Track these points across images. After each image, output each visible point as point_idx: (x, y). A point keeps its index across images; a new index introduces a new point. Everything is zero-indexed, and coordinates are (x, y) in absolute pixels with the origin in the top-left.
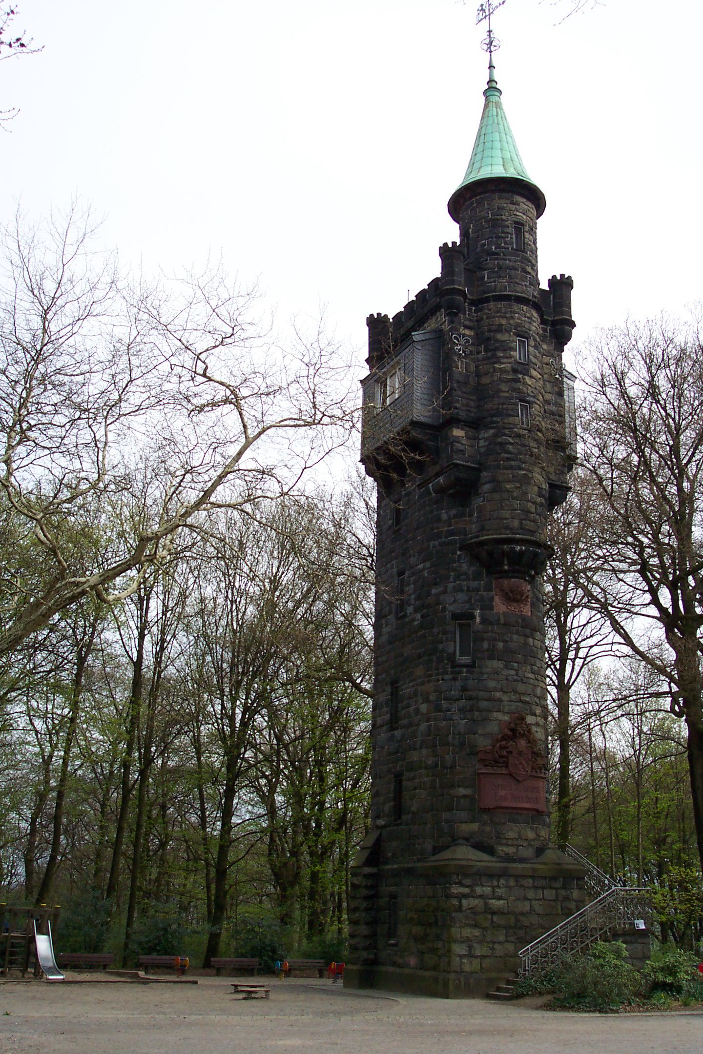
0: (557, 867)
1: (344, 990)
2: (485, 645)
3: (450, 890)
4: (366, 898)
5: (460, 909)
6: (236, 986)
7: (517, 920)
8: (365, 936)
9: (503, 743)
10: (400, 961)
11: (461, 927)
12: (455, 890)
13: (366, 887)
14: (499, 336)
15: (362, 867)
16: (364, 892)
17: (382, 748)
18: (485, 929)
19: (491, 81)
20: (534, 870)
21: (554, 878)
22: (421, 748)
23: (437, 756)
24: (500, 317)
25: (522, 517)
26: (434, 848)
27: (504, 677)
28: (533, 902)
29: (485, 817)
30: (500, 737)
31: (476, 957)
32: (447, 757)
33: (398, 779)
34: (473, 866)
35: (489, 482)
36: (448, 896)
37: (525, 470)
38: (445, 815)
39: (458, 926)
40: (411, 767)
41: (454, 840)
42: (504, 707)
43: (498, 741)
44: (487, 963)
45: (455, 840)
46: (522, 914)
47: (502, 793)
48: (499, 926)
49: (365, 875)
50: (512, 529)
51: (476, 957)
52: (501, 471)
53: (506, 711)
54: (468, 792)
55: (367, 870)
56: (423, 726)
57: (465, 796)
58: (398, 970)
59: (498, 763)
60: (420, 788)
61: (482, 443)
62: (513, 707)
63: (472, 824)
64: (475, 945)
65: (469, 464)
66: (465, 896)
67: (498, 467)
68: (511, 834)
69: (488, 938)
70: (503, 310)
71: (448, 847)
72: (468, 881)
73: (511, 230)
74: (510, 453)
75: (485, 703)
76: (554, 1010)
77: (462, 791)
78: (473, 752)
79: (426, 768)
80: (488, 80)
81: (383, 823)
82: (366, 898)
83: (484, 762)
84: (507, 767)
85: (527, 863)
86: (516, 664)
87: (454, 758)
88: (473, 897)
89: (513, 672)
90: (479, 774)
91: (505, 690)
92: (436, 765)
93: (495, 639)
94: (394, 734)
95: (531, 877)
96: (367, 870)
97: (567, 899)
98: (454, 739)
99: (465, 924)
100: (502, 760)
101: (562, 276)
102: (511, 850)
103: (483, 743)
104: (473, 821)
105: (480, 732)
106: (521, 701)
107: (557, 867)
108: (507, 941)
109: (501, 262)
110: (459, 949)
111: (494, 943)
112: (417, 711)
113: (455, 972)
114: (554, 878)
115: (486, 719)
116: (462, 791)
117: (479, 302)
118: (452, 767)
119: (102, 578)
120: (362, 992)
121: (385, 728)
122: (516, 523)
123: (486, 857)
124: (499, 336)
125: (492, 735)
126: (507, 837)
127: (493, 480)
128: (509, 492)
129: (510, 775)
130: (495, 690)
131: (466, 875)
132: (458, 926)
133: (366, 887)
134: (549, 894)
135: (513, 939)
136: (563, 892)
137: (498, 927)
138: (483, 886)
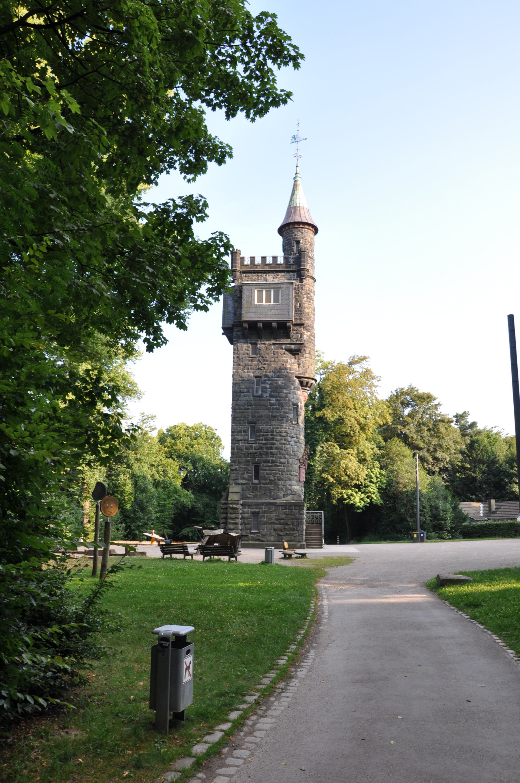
26: (284, 495)
38: (288, 483)
127: (310, 353)
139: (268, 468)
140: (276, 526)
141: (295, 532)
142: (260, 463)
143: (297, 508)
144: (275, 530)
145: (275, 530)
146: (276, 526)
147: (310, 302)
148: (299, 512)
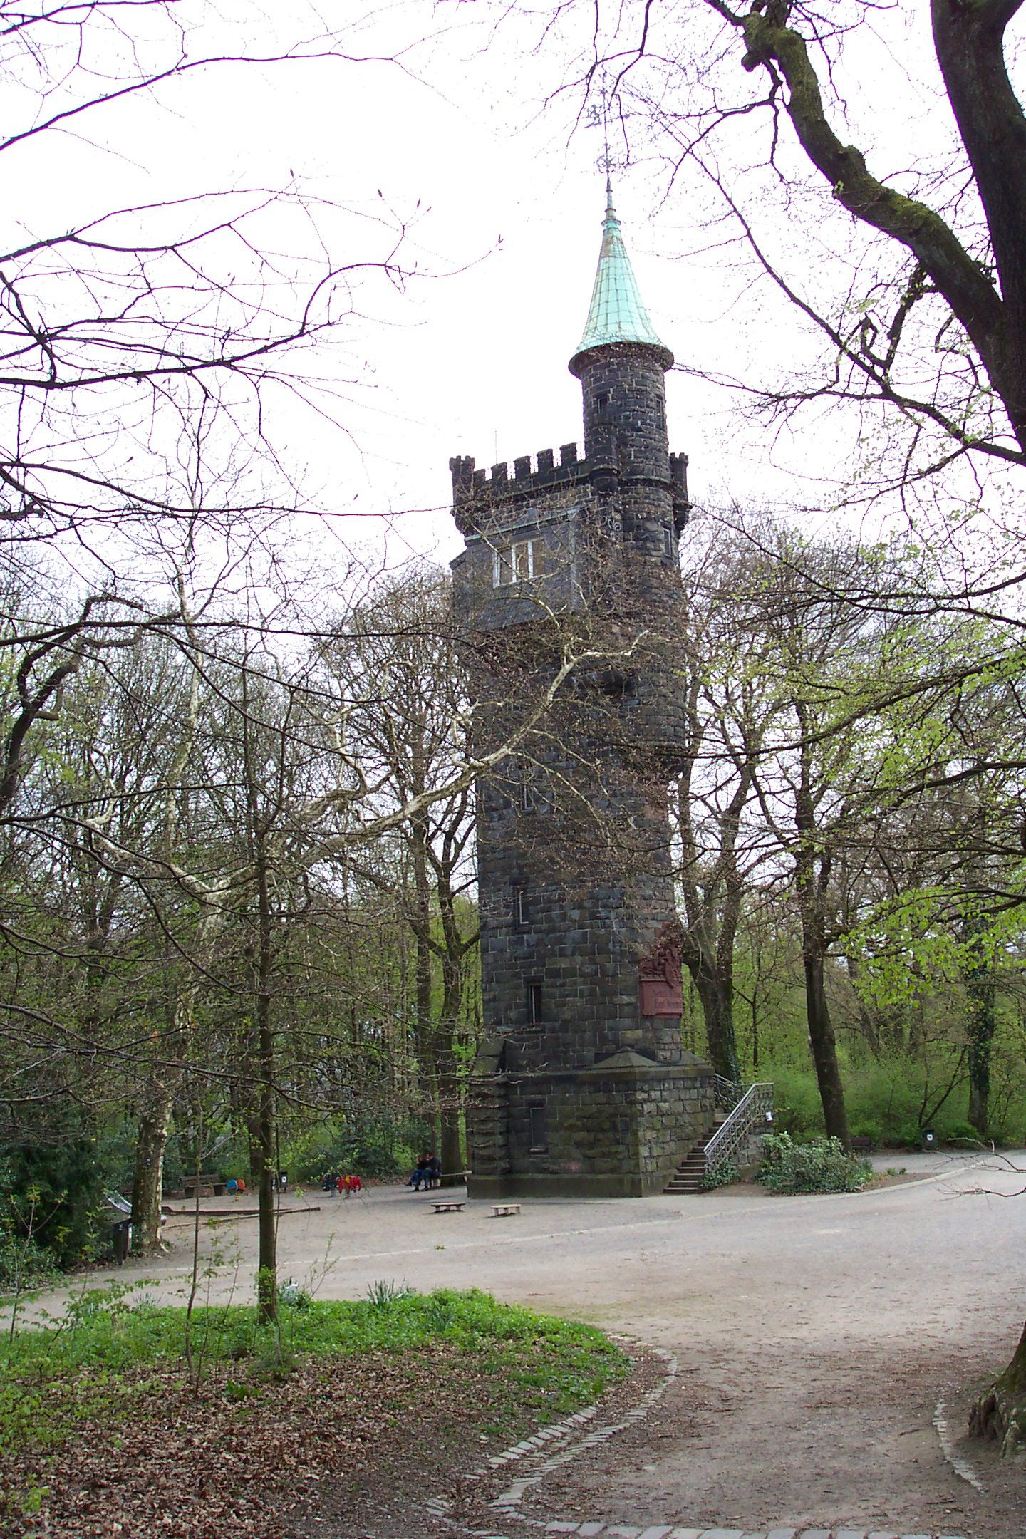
0: (694, 1068)
6: (438, 1207)
8: (500, 1146)
12: (641, 1096)
14: (648, 525)
17: (502, 951)
18: (658, 1130)
19: (609, 209)
21: (695, 1079)
22: (573, 954)
23: (595, 963)
24: (648, 503)
26: (597, 1055)
32: (608, 965)
33: (535, 986)
34: (648, 1072)
36: (632, 1103)
38: (607, 1024)
40: (555, 973)
41: (618, 1047)
45: (620, 1047)
46: (679, 1114)
47: (661, 1000)
54: (632, 999)
56: (576, 933)
58: (555, 1177)
66: (645, 1101)
68: (667, 1040)
70: (651, 497)
71: (613, 1054)
72: (646, 1087)
73: (653, 404)
77: (626, 999)
78: (635, 959)
79: (581, 976)
80: (606, 208)
83: (645, 970)
84: (664, 974)
98: (614, 947)
101: (682, 454)
102: (668, 1054)
109: (649, 441)
110: (644, 1151)
112: (564, 917)
114: (695, 1079)
116: (626, 999)
117: (627, 484)
118: (615, 975)
121: (504, 929)
123: (650, 1063)
124: (648, 525)
129: (667, 982)
131: (645, 1082)
134: (694, 1093)
135: (674, 1138)
137: (665, 1127)
140: (578, 1136)
141: (621, 1148)
142: (540, 979)
144: (578, 1145)
145: (578, 1145)
146: (578, 1136)
147: (643, 548)
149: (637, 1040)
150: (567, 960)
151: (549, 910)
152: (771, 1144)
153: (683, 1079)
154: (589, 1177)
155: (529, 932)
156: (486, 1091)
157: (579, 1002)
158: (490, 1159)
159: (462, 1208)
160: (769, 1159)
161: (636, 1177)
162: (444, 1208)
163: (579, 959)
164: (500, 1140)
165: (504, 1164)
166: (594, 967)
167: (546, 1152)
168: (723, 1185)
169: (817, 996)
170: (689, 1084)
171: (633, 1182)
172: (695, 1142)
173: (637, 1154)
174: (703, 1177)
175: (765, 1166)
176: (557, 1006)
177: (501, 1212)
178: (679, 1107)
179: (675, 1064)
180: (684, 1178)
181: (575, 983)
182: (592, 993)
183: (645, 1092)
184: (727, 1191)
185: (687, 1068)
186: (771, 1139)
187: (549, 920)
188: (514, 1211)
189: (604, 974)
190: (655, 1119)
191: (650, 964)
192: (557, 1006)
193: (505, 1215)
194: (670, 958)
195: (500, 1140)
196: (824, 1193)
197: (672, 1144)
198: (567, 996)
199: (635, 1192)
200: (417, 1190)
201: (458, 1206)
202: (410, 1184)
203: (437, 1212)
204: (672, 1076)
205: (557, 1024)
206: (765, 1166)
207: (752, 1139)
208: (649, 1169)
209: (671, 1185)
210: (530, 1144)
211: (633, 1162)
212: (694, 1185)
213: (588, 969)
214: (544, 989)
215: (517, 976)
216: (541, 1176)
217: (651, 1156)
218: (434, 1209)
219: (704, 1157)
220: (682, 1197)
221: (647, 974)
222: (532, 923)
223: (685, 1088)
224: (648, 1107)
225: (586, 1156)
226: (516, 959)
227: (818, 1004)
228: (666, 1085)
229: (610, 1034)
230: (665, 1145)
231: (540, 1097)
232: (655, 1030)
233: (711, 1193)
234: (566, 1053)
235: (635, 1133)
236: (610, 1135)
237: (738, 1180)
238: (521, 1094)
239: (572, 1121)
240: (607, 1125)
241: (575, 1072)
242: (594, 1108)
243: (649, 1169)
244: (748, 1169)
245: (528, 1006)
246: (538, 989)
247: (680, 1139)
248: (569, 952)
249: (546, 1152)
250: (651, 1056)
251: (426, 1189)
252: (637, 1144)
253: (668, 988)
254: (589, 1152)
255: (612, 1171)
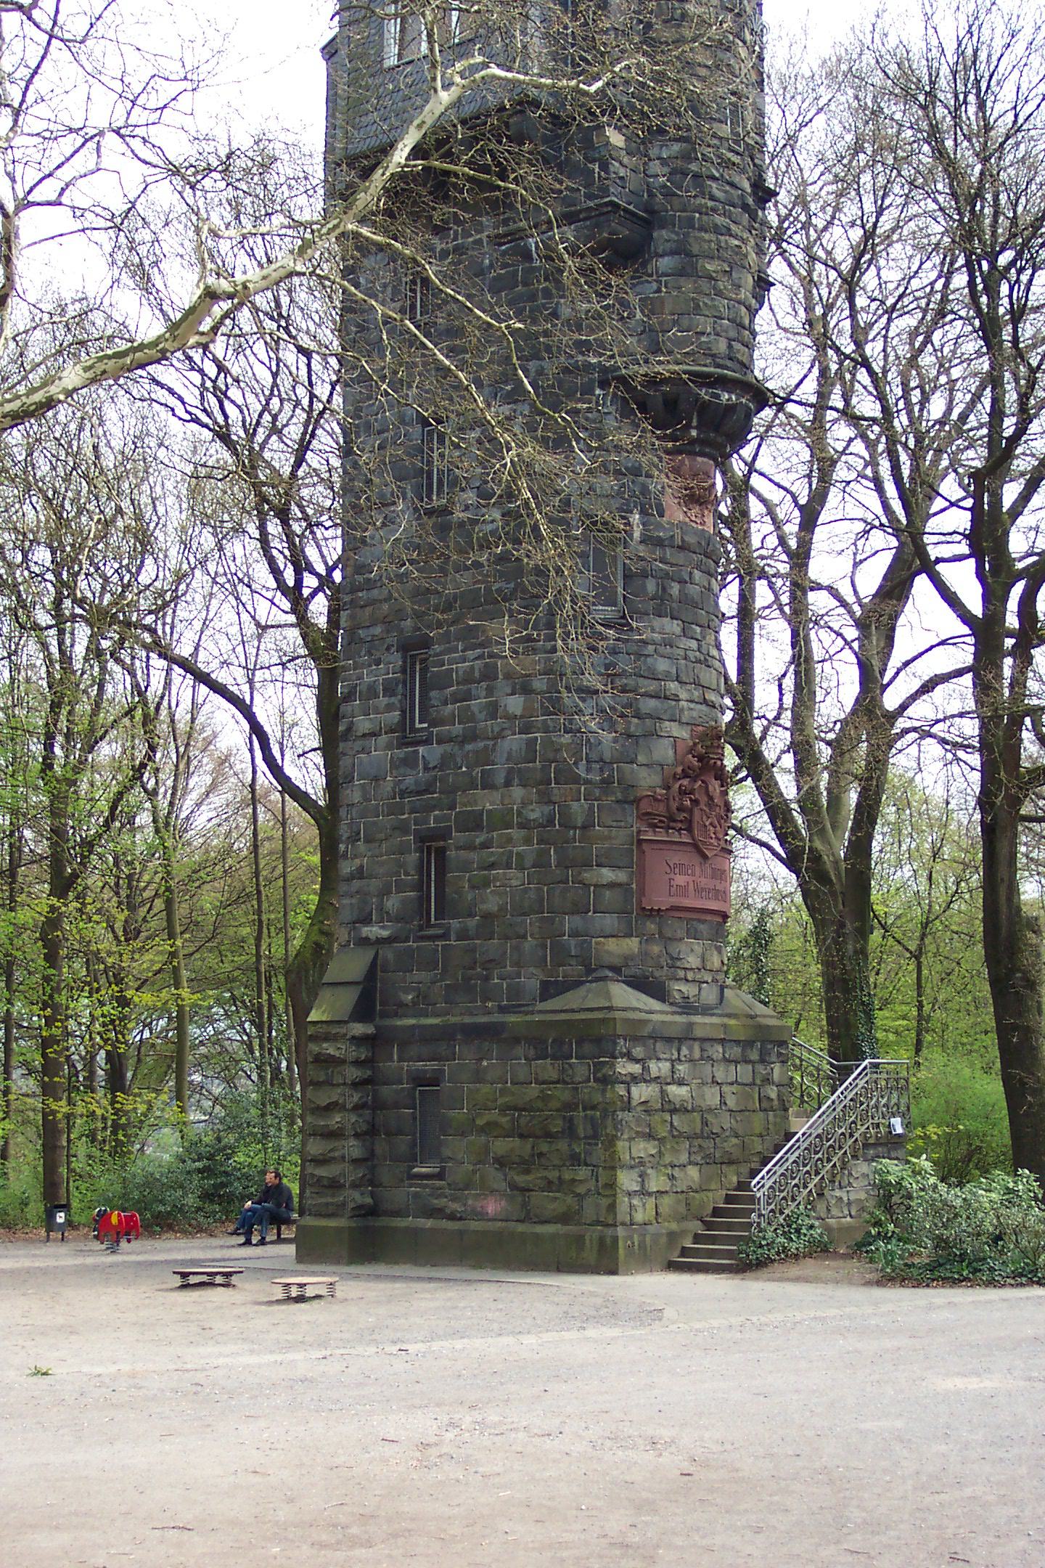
0: (750, 1022)
1: (301, 1267)
2: (651, 586)
3: (613, 1066)
4: (356, 1085)
5: (627, 1106)
6: (184, 1275)
7: (705, 1123)
8: (355, 1161)
9: (685, 782)
10: (456, 1206)
11: (631, 1139)
12: (625, 1068)
13: (357, 1063)
15: (346, 1022)
16: (353, 1073)
18: (662, 1141)
20: (725, 1026)
22: (508, 784)
25: (732, 334)
26: (545, 985)
27: (682, 653)
28: (726, 1089)
29: (651, 927)
30: (679, 770)
31: (650, 1194)
34: (646, 1022)
35: (672, 253)
37: (736, 237)
38: (568, 922)
39: (626, 1136)
40: (473, 822)
41: (589, 971)
42: (682, 710)
43: (675, 777)
44: (666, 1201)
45: (593, 970)
46: (710, 1110)
47: (680, 880)
48: (681, 1134)
49: (353, 1038)
50: (713, 356)
51: (650, 1194)
52: (697, 234)
53: (684, 720)
54: (621, 876)
55: (359, 1029)
56: (514, 742)
57: (612, 885)
59: (675, 821)
60: (509, 866)
61: (655, 167)
62: (695, 714)
63: (627, 940)
64: (649, 1171)
65: (631, 207)
66: (635, 1079)
67: (690, 223)
68: (693, 961)
69: (668, 1159)
71: (578, 984)
72: (638, 1051)
74: (712, 198)
75: (652, 703)
76: (928, 1286)
77: (608, 875)
78: (630, 799)
79: (522, 826)
81: (385, 933)
82: (356, 1085)
84: (690, 830)
85: (713, 1015)
86: (698, 629)
87: (591, 808)
88: (645, 1081)
89: (694, 644)
90: (640, 842)
91: (684, 679)
92: (551, 822)
93: (667, 575)
94: (417, 752)
95: (722, 1041)
96: (359, 1029)
97: (767, 1080)
98: (588, 770)
99: (637, 1133)
100: (682, 816)
103: (647, 780)
104: (629, 935)
105: (641, 759)
106: (705, 702)
107: (750, 1022)
108: (690, 1163)
110: (627, 1180)
111: (673, 1166)
112: (493, 710)
113: (623, 1224)
114: (748, 1044)
115: (653, 734)
116: (608, 875)
118: (586, 827)
119: (90, 375)
120: (354, 1269)
121: (384, 738)
122: (722, 346)
125: (662, 765)
126: (688, 966)
127: (681, 250)
128: (712, 278)
130: (667, 677)
131: (636, 1039)
132: (626, 1136)
133: (357, 1063)
134: (744, 1072)
135: (698, 1159)
136: (761, 1069)
137: (676, 1135)
138: (659, 1059)
139: (474, 856)
140: (501, 1146)
141: (583, 1173)
142: (444, 834)
143: (587, 1048)
144: (501, 1162)
145: (501, 1162)
146: (501, 1146)
148: (599, 1066)
149: (628, 958)
150: (497, 795)
151: (468, 697)
152: (892, 1179)
153: (722, 1041)
154: (521, 1228)
155: (427, 742)
156: (331, 1051)
157: (516, 878)
158: (334, 1185)
159: (234, 1279)
160: (889, 1209)
161: (609, 1232)
162: (205, 1278)
163: (518, 792)
164: (353, 1148)
165: (359, 1198)
166: (547, 809)
167: (440, 1176)
168: (788, 1256)
169: (1003, 891)
170: (736, 1051)
171: (602, 1241)
172: (744, 1169)
173: (612, 1185)
174: (748, 1240)
175: (878, 1223)
176: (473, 887)
177: (294, 1292)
178: (711, 1097)
179: (706, 1010)
180: (713, 1239)
181: (509, 840)
182: (541, 862)
183: (637, 1061)
184: (794, 1270)
185: (732, 1022)
186: (893, 1169)
187: (467, 717)
188: (323, 1291)
189: (567, 825)
190: (657, 1118)
191: (661, 809)
192: (473, 887)
193: (301, 1299)
194: (703, 799)
195: (353, 1148)
196: (991, 1283)
197: (693, 1172)
198: (492, 866)
199: (606, 1262)
200: (248, 1242)
201: (228, 1275)
202: (235, 1233)
203: (185, 1287)
204: (699, 1033)
205: (472, 923)
206: (878, 1223)
207: (862, 1168)
208: (639, 1217)
209: (685, 1252)
210: (413, 1159)
211: (605, 1202)
212: (729, 1254)
213: (535, 813)
214: (451, 854)
215: (403, 828)
216: (429, 1223)
217: (644, 1192)
218: (178, 1281)
219: (752, 1199)
220: (700, 1278)
221: (654, 826)
222: (433, 723)
223: (727, 1061)
224: (640, 1093)
225: (513, 1186)
226: (403, 794)
227: (1004, 909)
228: (685, 1051)
229: (573, 942)
230: (677, 1172)
231: (431, 1066)
232: (667, 940)
233: (759, 1273)
234: (487, 979)
235: (612, 1141)
236: (562, 1145)
237: (821, 1249)
238: (400, 1060)
239: (494, 1115)
240: (557, 1126)
241: (497, 1018)
242: (533, 1090)
243: (639, 1217)
244: (848, 1229)
245: (421, 886)
246: (441, 853)
247: (709, 1160)
248: (500, 779)
249: (440, 1176)
250: (656, 990)
251: (262, 1242)
252: (613, 1166)
253: (697, 859)
254: (521, 1180)
255: (565, 1218)
